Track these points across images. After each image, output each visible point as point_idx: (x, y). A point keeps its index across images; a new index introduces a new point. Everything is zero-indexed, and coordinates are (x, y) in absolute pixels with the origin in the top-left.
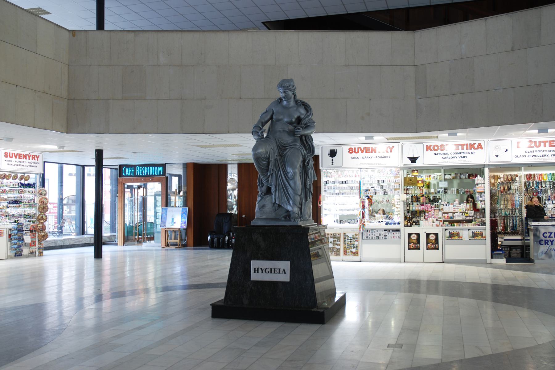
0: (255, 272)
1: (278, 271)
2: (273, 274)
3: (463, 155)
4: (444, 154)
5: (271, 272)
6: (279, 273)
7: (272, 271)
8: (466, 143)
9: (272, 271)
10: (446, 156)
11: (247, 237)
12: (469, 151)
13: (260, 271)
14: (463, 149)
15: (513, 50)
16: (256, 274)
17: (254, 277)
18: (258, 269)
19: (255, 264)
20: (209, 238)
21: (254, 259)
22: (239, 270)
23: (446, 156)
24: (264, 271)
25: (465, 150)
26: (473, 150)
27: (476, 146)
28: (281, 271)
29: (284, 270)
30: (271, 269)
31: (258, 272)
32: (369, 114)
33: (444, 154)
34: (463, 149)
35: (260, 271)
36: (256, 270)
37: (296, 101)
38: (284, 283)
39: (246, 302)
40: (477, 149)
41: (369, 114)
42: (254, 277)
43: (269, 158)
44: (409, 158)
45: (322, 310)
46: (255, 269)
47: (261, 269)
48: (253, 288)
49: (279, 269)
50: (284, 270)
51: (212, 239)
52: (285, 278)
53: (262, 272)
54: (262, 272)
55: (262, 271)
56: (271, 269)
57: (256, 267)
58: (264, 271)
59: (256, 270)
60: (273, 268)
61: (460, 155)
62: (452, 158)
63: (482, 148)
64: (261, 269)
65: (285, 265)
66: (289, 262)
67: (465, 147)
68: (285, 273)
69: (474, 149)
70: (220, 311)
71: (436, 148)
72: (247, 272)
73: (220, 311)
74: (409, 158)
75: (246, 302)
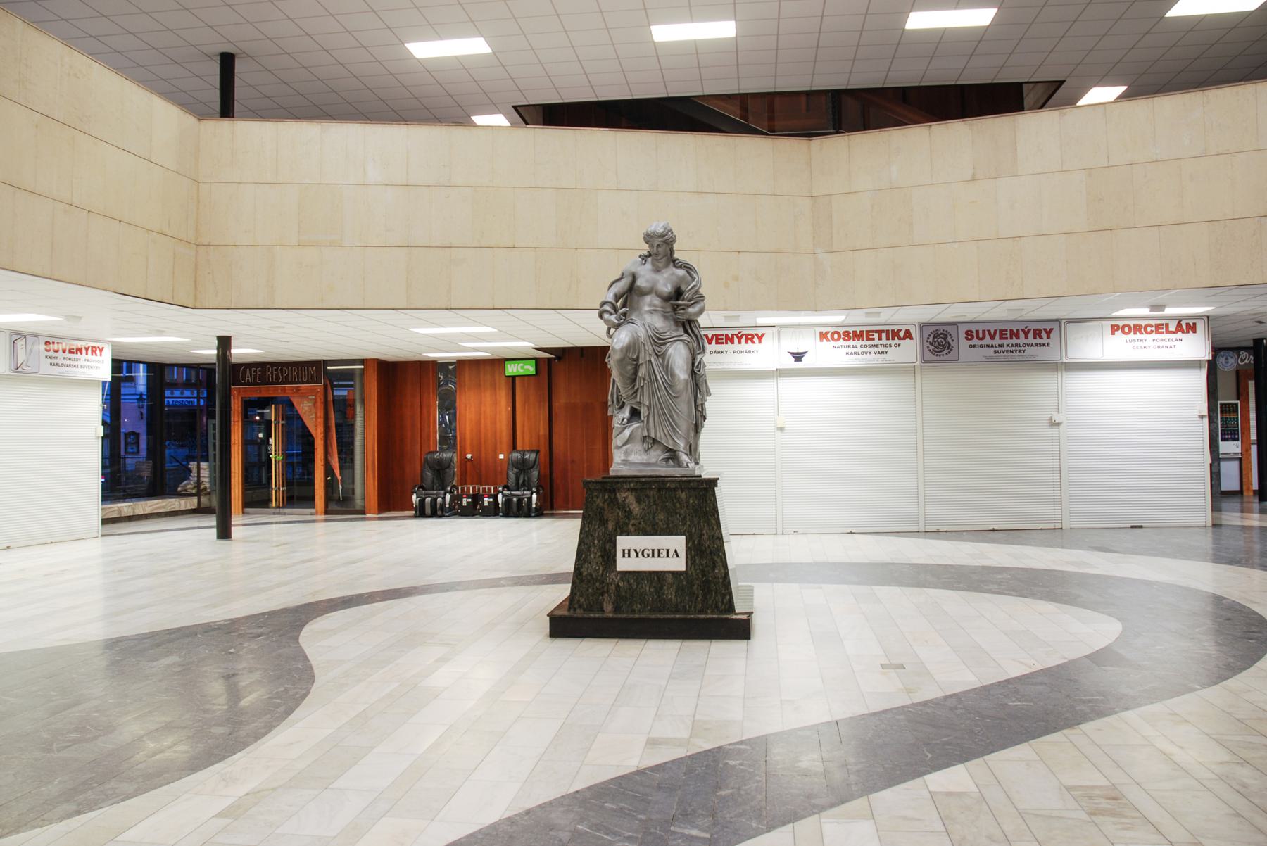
1: (665, 553)
3: (880, 349)
7: (653, 553)
8: (885, 328)
9: (653, 553)
10: (853, 350)
12: (891, 342)
13: (633, 554)
14: (880, 339)
15: (973, 179)
16: (627, 559)
17: (623, 564)
19: (623, 542)
20: (414, 497)
22: (595, 552)
23: (853, 350)
25: (884, 341)
26: (897, 341)
27: (902, 334)
28: (671, 553)
32: (736, 278)
34: (880, 339)
35: (633, 554)
36: (626, 553)
39: (608, 607)
40: (904, 338)
41: (736, 278)
42: (623, 564)
43: (637, 359)
45: (745, 617)
48: (621, 584)
51: (422, 502)
52: (679, 564)
57: (626, 548)
59: (626, 553)
61: (876, 349)
62: (863, 353)
63: (911, 338)
65: (678, 542)
67: (884, 335)
69: (900, 338)
70: (564, 625)
71: (836, 336)
72: (609, 557)
73: (564, 625)
75: (608, 607)
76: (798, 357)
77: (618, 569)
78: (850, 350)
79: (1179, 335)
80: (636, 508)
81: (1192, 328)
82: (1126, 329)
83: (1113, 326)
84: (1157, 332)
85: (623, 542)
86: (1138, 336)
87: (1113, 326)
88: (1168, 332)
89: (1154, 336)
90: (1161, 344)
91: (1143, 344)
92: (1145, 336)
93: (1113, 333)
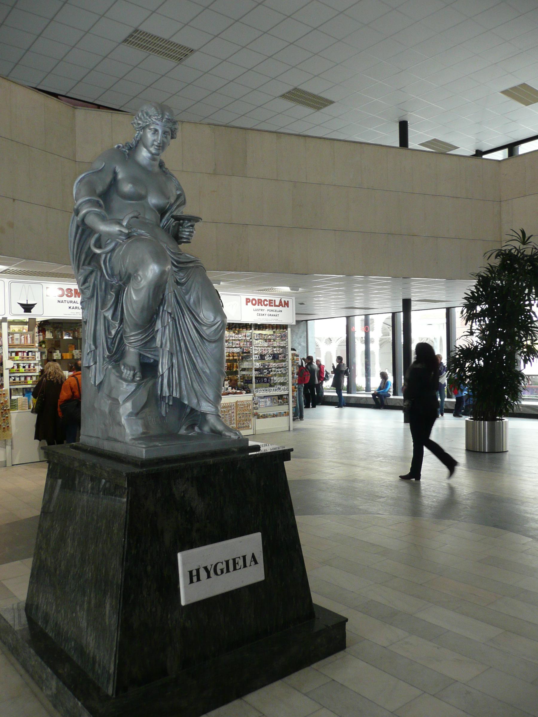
0: (191, 582)
1: (241, 562)
2: (232, 574)
4: (71, 302)
5: (228, 571)
6: (245, 566)
11: (159, 495)
16: (196, 584)
18: (198, 571)
21: (182, 550)
24: (212, 572)
28: (249, 559)
29: (253, 556)
30: (227, 562)
31: (199, 580)
33: (71, 302)
36: (194, 577)
37: (161, 165)
38: (252, 588)
44: (22, 305)
46: (191, 572)
47: (206, 568)
49: (244, 557)
50: (253, 556)
53: (209, 577)
54: (209, 577)
55: (208, 572)
56: (227, 562)
57: (194, 567)
58: (212, 572)
59: (194, 577)
60: (230, 558)
64: (206, 568)
65: (252, 543)
66: (259, 534)
68: (256, 563)
74: (22, 305)
76: (28, 308)
77: (183, 603)
78: (72, 305)
79: (281, 308)
80: (199, 505)
81: (287, 304)
82: (254, 302)
83: (247, 299)
84: (270, 306)
85: (186, 561)
86: (260, 307)
87: (247, 299)
88: (275, 306)
89: (268, 307)
90: (272, 313)
91: (262, 313)
92: (263, 307)
93: (247, 304)
